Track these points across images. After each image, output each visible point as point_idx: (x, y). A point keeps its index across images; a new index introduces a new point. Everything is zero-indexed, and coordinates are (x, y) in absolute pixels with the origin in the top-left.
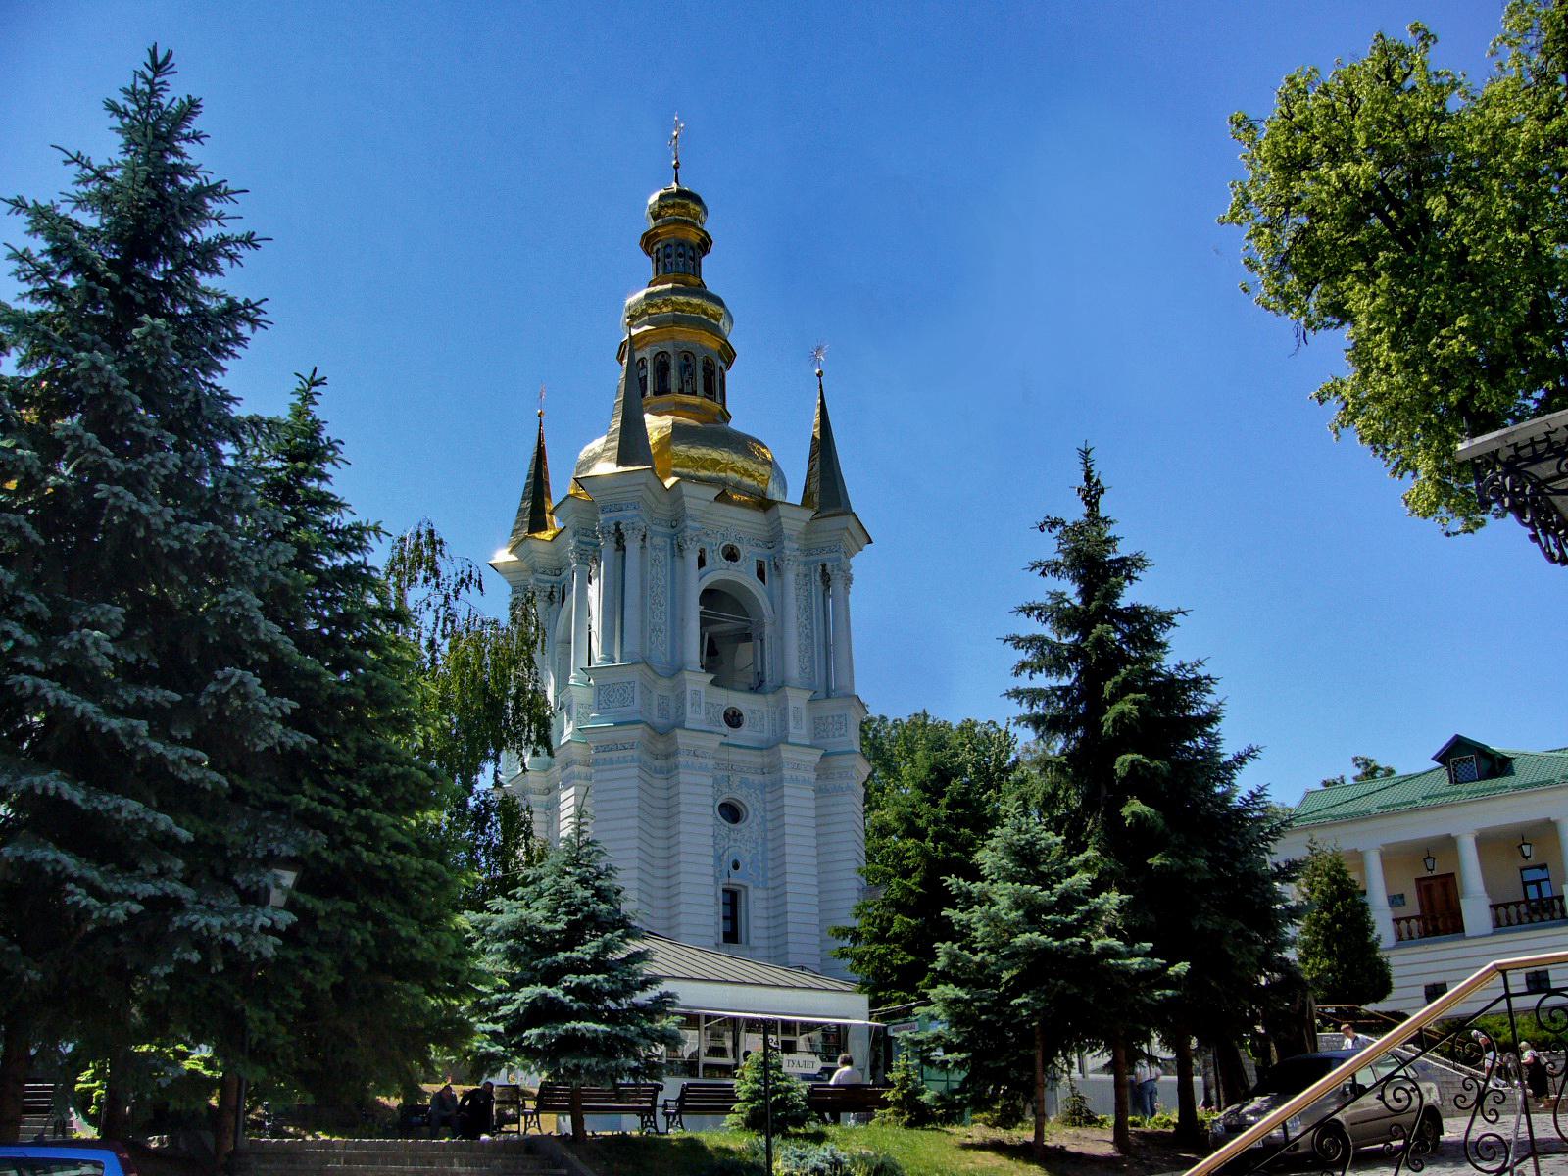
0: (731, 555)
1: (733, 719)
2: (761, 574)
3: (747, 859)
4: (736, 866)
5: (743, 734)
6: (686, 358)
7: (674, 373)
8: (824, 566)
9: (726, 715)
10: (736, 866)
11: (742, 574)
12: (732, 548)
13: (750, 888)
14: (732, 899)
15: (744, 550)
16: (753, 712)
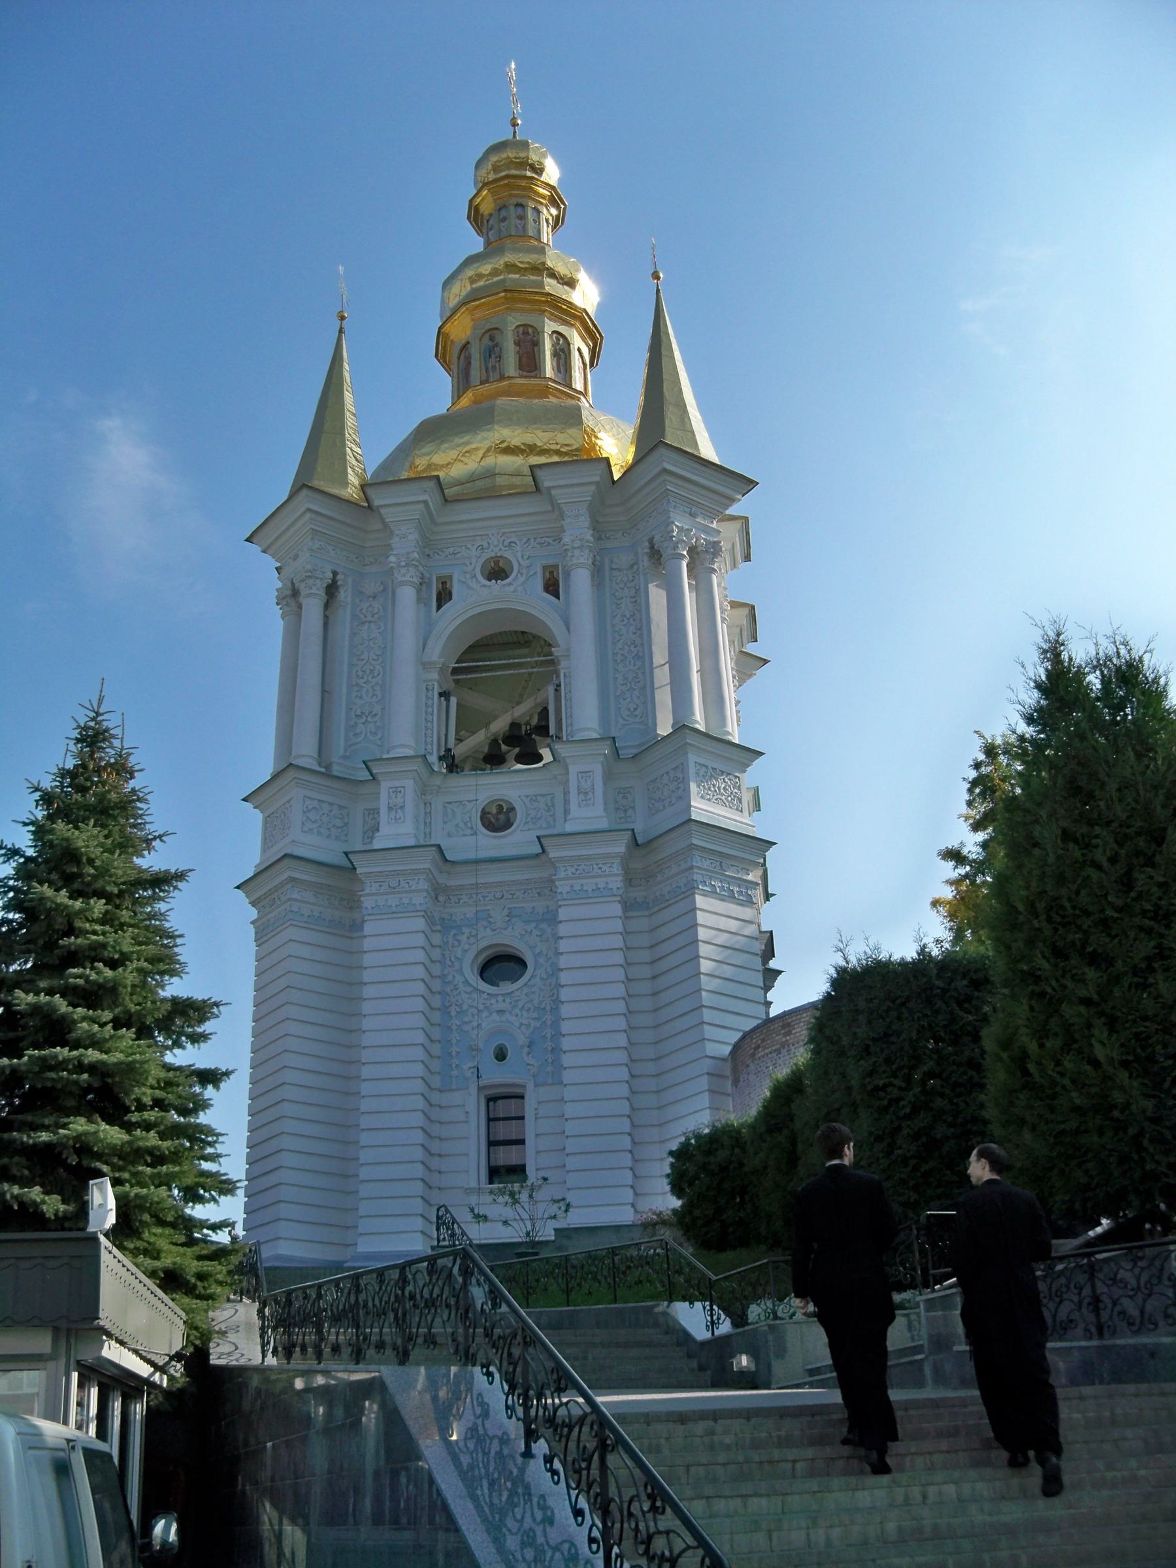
0: (497, 572)
1: (498, 819)
2: (552, 587)
3: (522, 1040)
4: (501, 1055)
5: (518, 840)
6: (492, 339)
7: (476, 364)
8: (651, 541)
9: (484, 815)
10: (501, 1055)
11: (523, 596)
12: (496, 560)
13: (530, 1086)
14: (502, 1106)
15: (515, 557)
16: (534, 799)
